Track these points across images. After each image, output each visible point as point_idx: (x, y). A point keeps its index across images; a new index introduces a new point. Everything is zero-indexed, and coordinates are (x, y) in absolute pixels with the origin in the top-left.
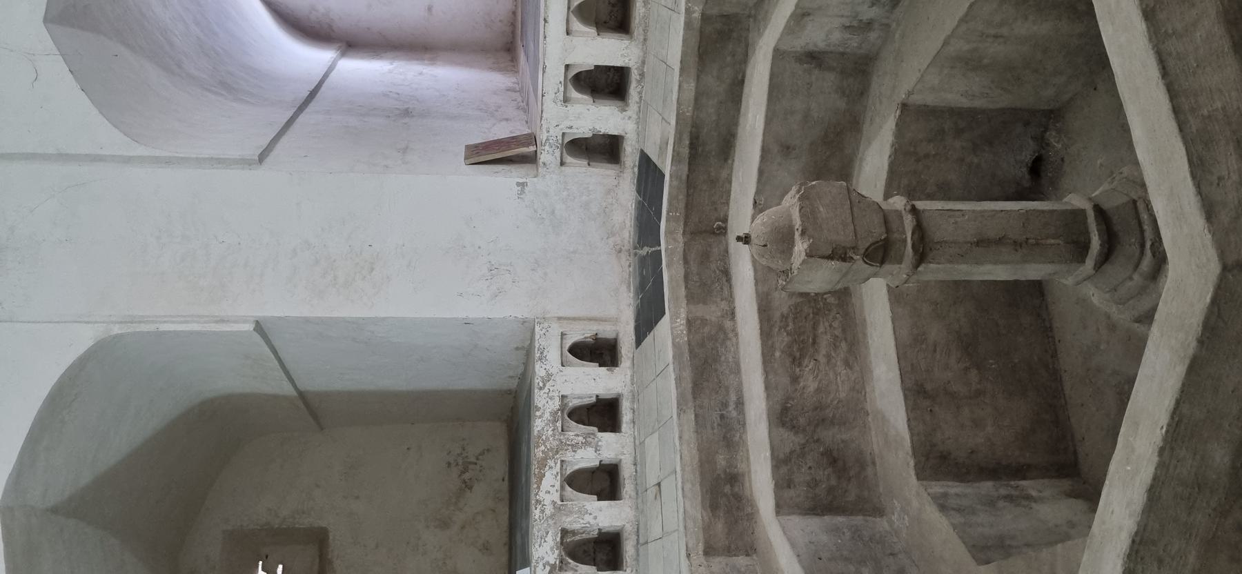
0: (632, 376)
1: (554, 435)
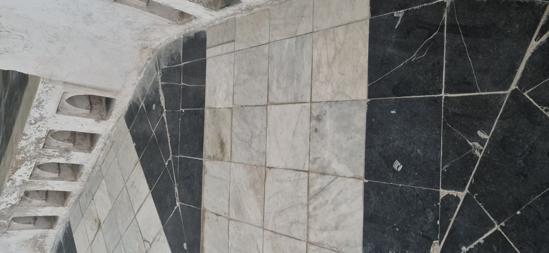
0: (114, 127)
1: (35, 150)
